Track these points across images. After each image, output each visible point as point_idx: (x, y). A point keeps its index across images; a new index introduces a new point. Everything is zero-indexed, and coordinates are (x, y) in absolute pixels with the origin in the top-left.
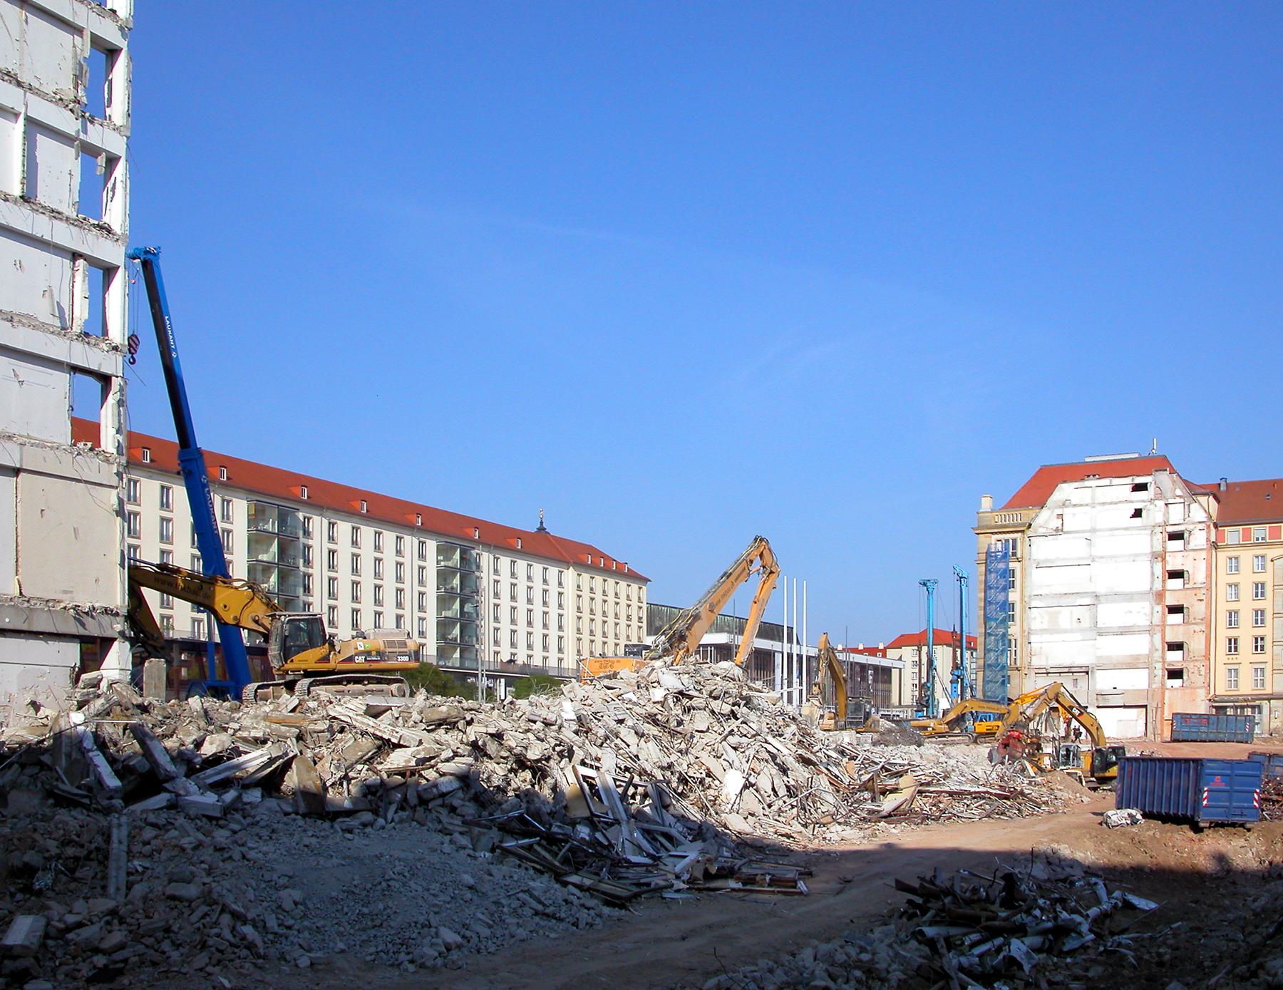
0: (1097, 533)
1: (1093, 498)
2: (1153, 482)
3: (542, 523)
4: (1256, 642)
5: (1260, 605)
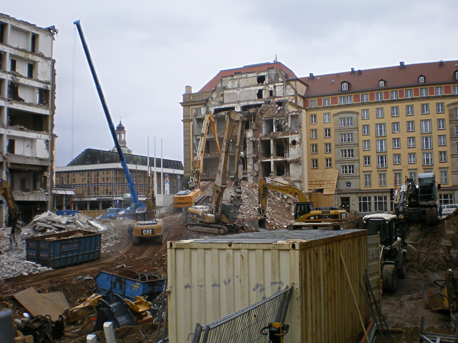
0: (241, 104)
1: (239, 85)
2: (268, 75)
3: (120, 122)
4: (327, 162)
5: (328, 141)
